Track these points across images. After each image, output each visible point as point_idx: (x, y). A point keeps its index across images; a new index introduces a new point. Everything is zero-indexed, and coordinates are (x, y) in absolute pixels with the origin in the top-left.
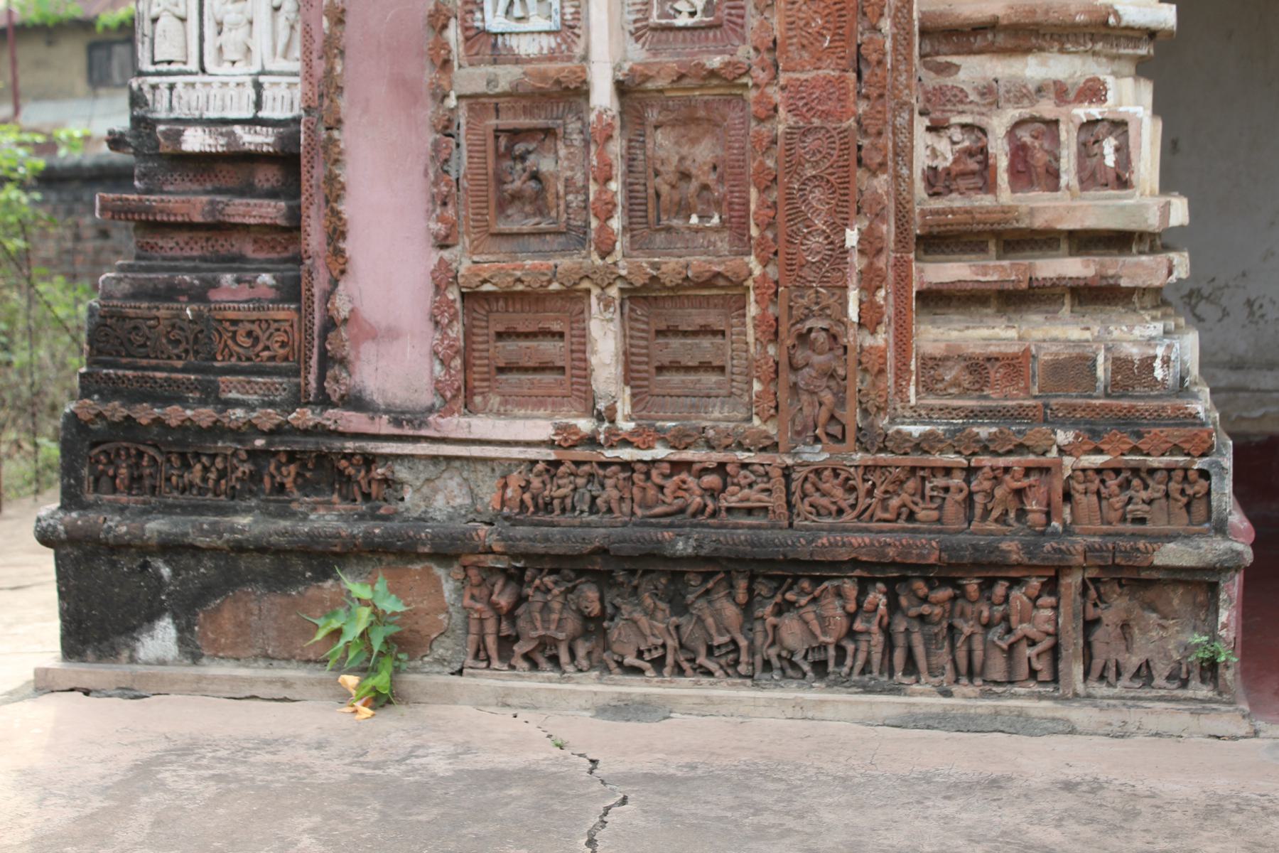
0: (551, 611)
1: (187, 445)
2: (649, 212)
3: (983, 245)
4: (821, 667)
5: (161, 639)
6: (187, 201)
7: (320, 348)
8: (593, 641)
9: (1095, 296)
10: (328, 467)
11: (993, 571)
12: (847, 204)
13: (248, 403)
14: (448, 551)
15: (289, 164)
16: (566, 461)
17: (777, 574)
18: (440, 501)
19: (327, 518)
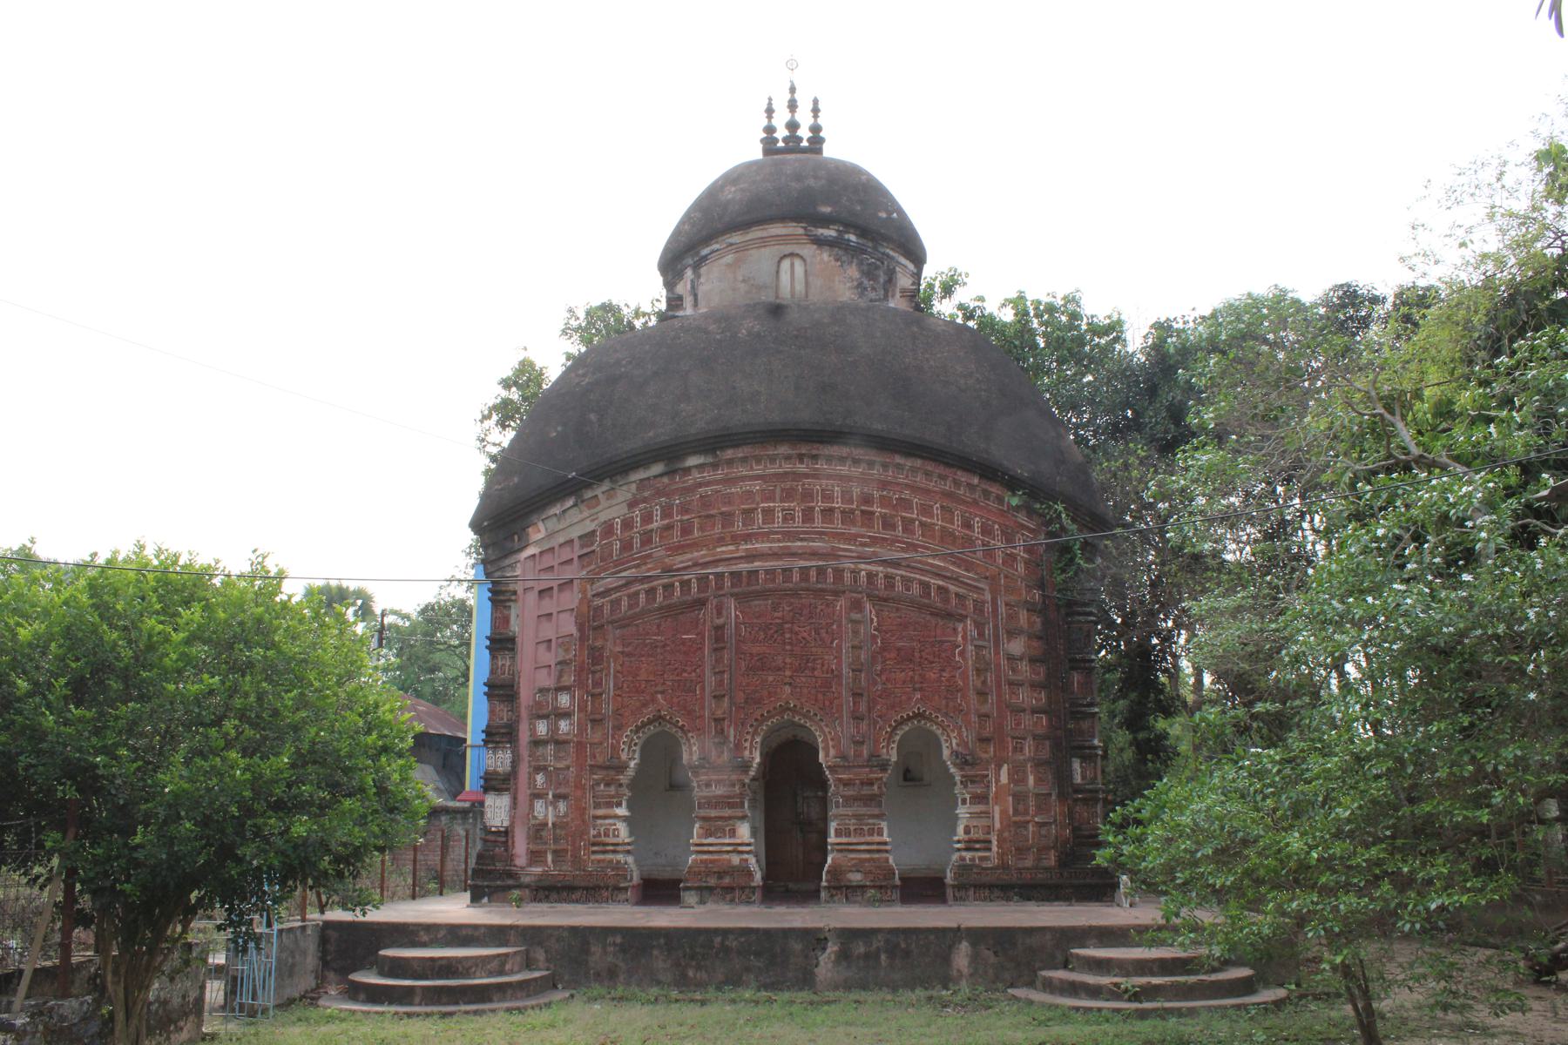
0: (541, 894)
1: (490, 872)
2: (556, 840)
3: (599, 845)
4: (577, 901)
5: (485, 900)
6: (492, 838)
7: (511, 857)
8: (547, 899)
9: (614, 852)
10: (511, 875)
11: (600, 888)
12: (582, 839)
13: (499, 866)
14: (527, 886)
15: (507, 833)
16: (545, 874)
17: (571, 889)
18: (526, 880)
19: (510, 882)
